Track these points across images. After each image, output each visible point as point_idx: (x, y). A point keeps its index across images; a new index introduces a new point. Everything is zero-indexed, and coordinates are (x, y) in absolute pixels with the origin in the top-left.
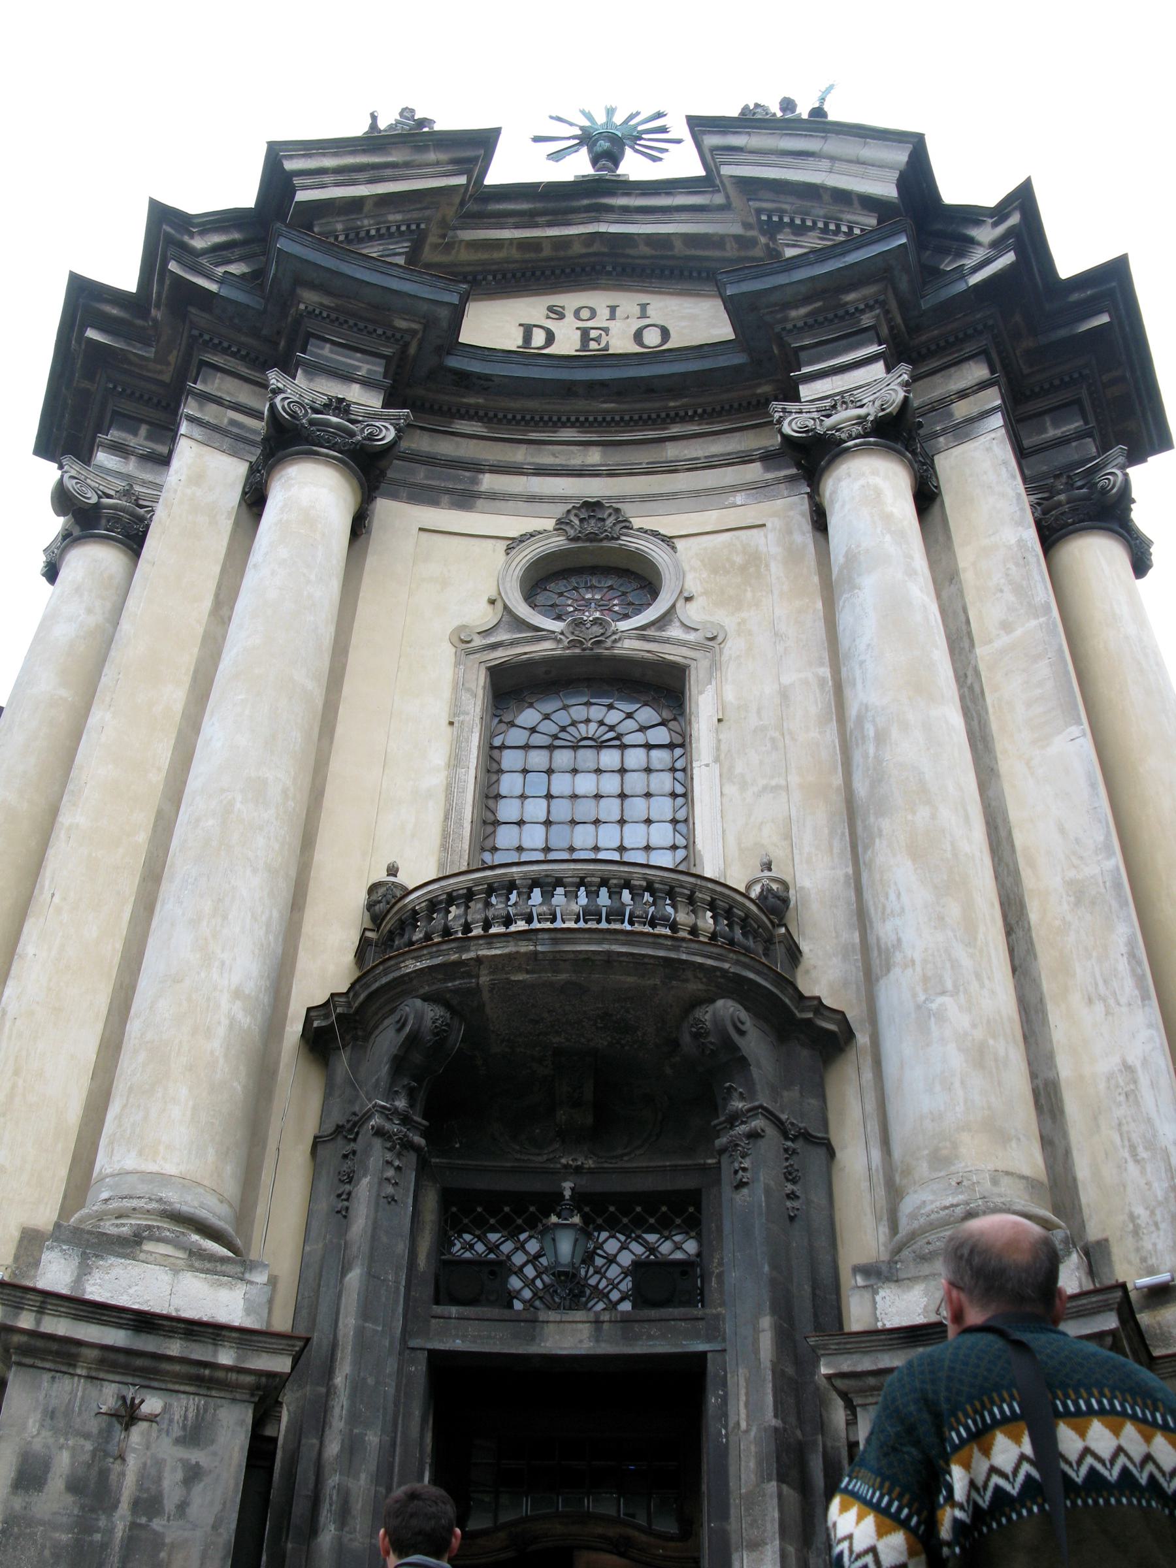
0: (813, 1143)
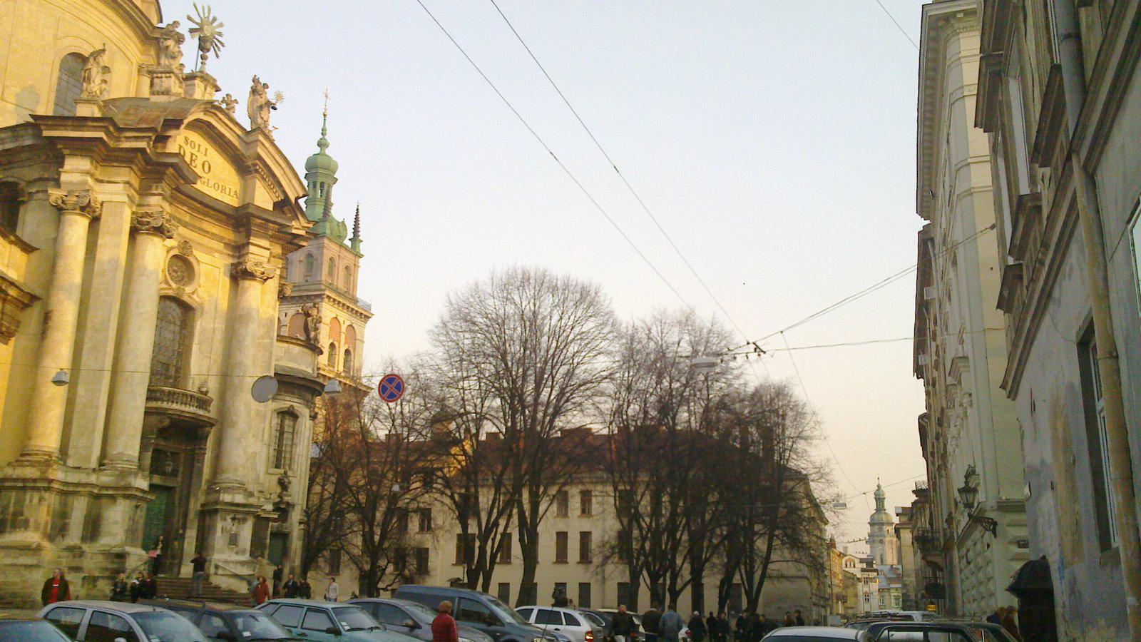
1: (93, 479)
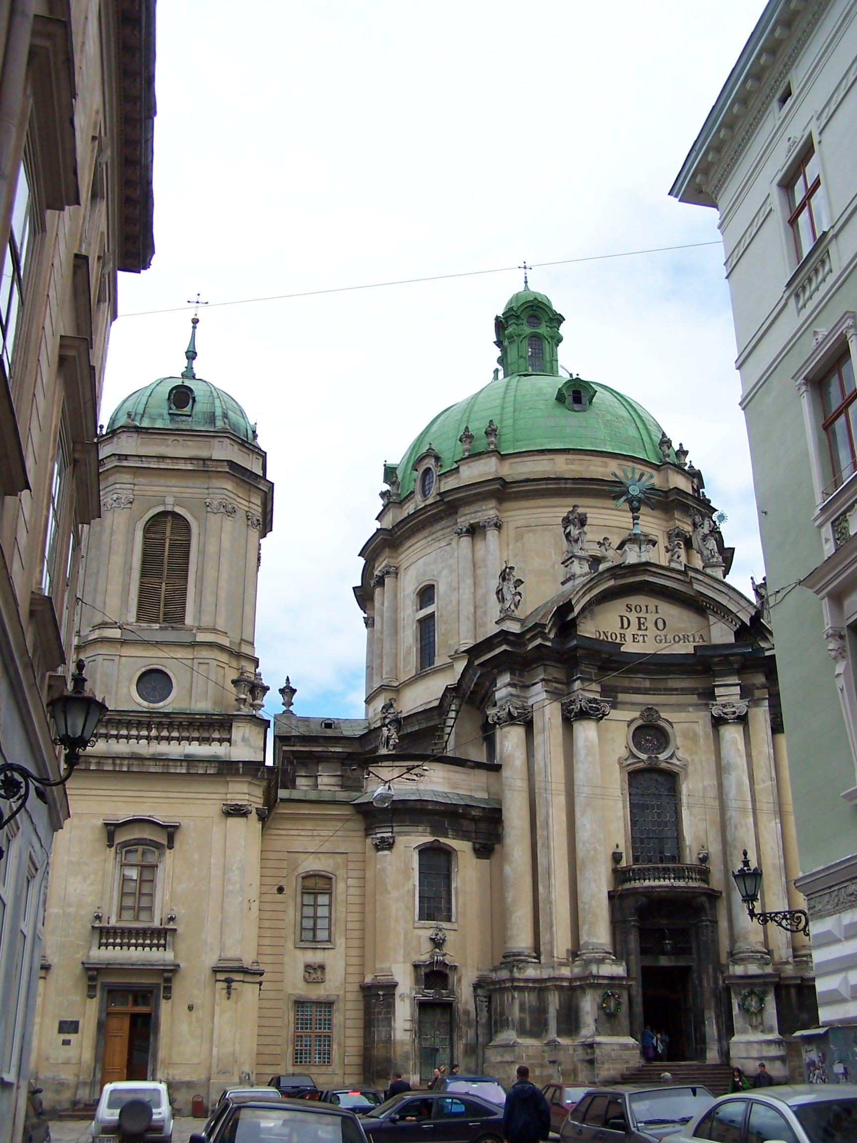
0: (715, 922)
1: (566, 972)
